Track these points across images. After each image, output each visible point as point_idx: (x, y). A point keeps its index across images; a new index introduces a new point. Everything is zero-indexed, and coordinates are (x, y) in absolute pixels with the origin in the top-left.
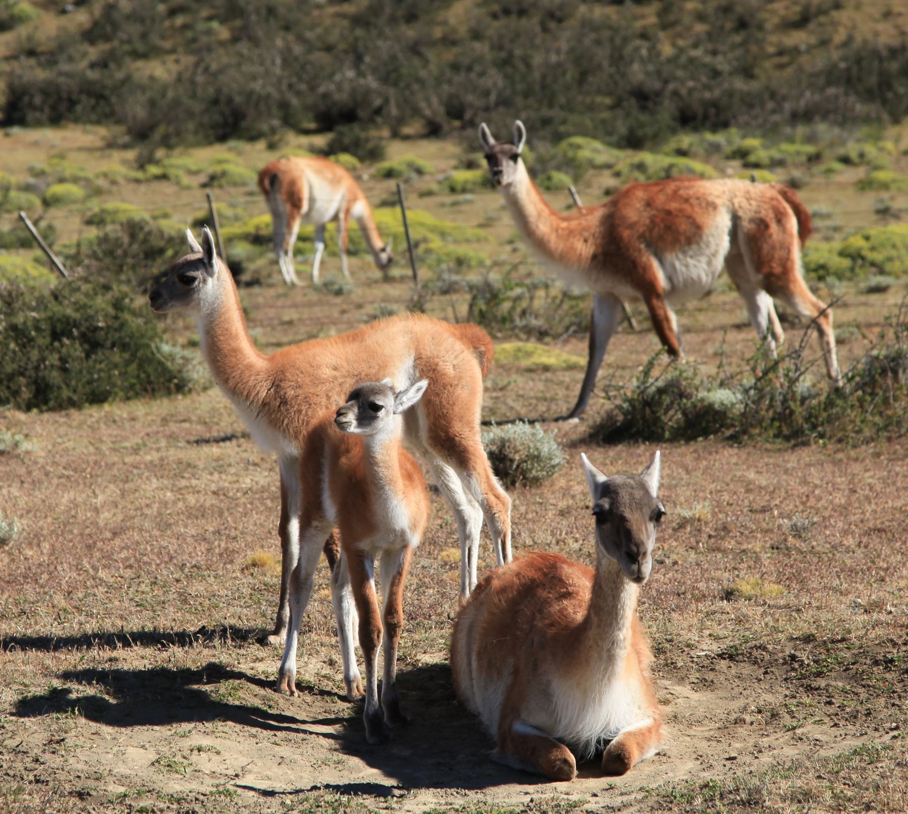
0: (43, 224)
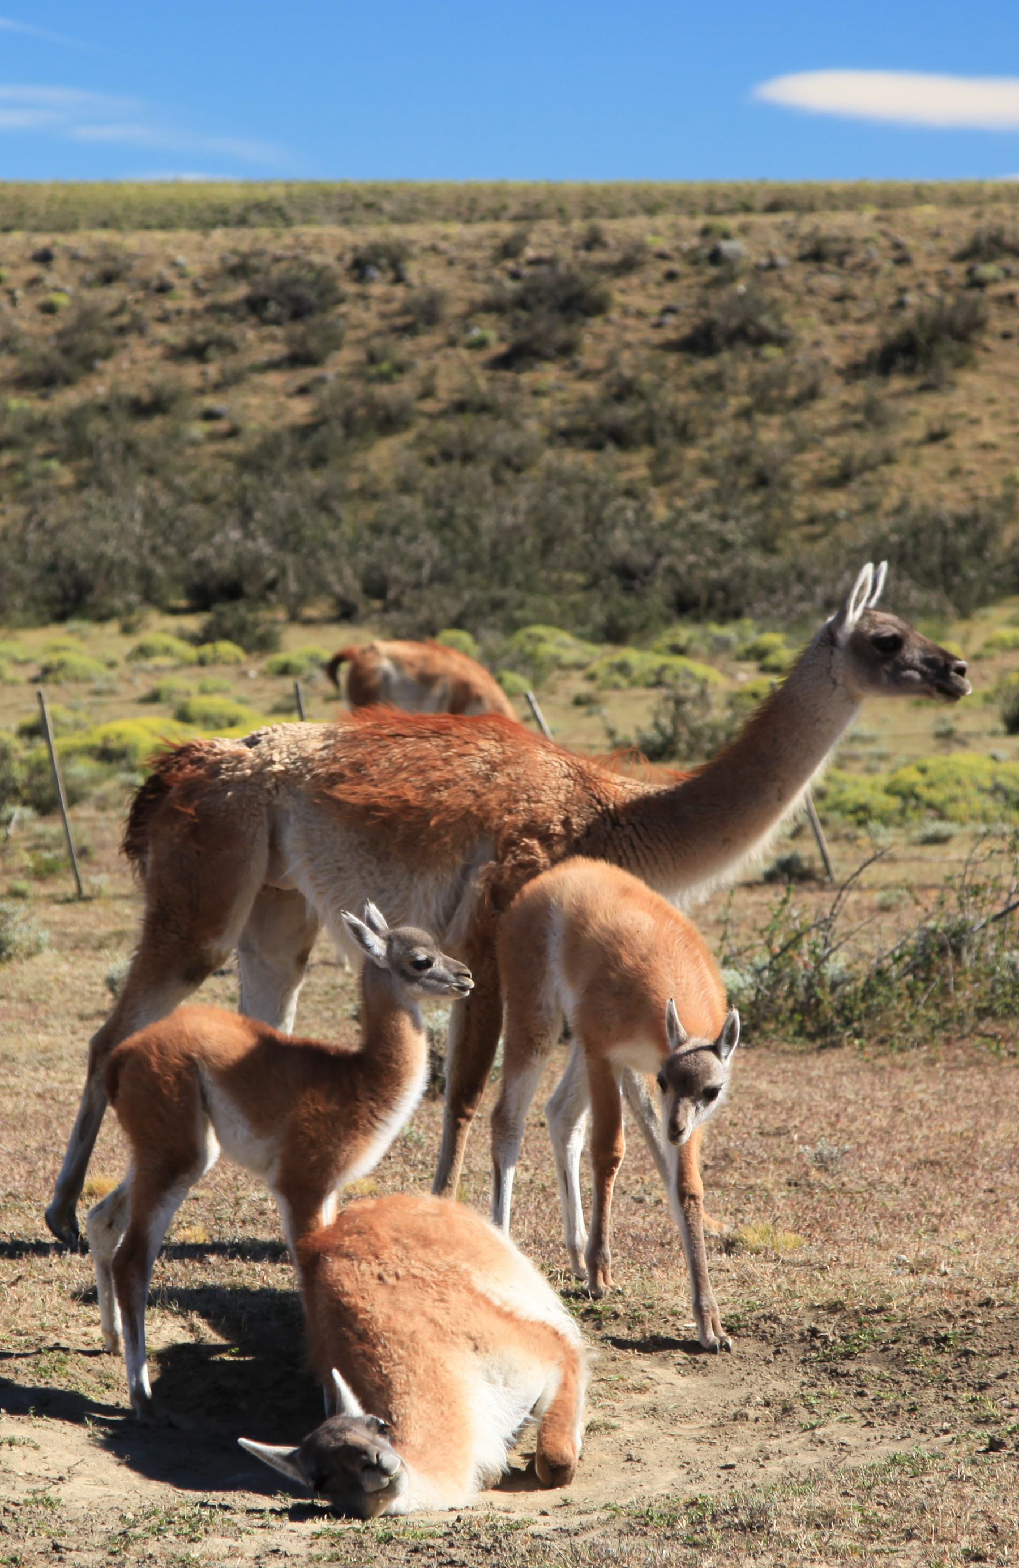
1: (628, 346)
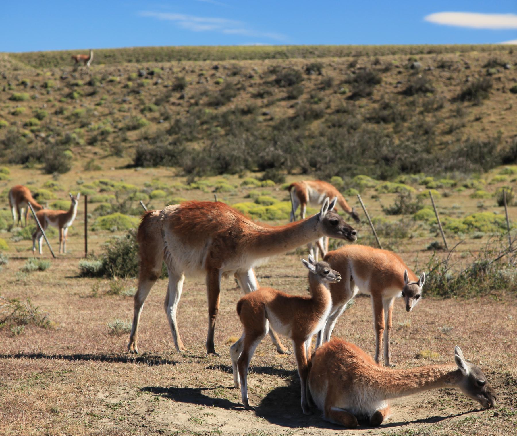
0: (149, 206)
1: (387, 93)
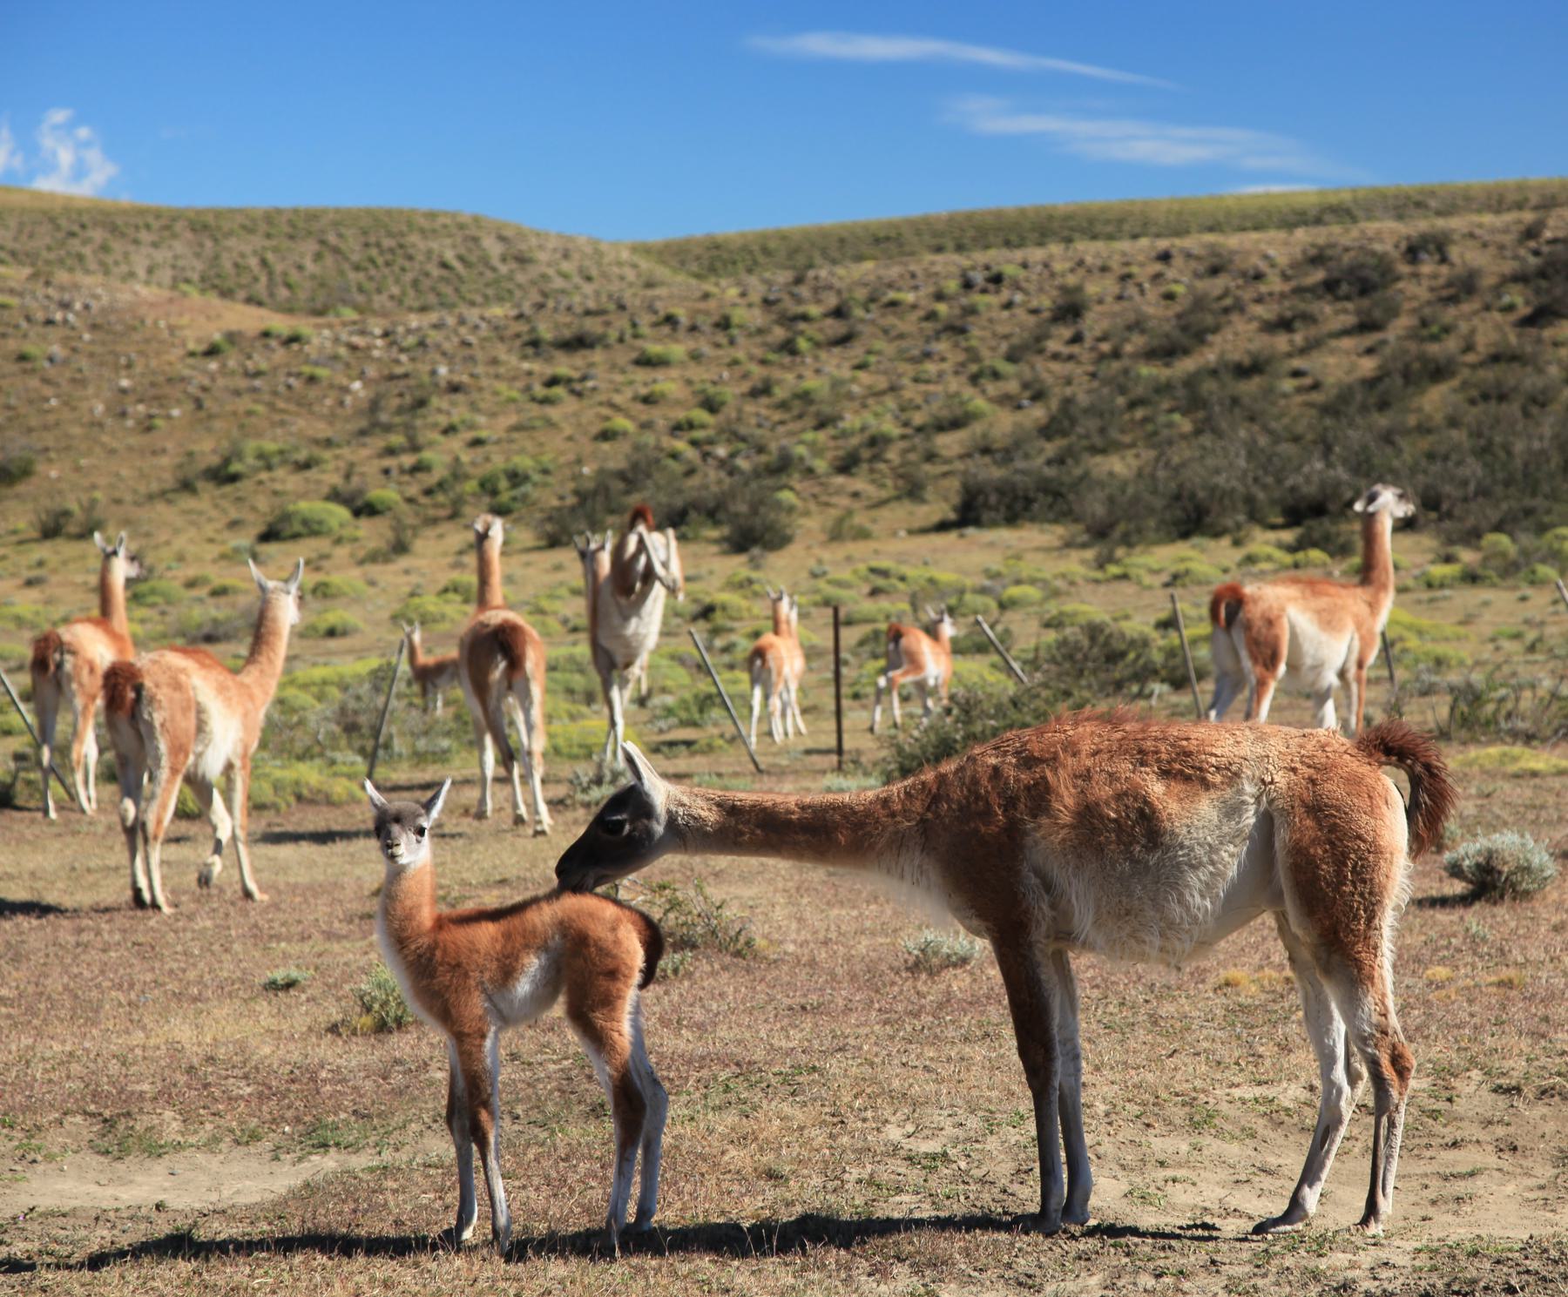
0: (999, 628)
